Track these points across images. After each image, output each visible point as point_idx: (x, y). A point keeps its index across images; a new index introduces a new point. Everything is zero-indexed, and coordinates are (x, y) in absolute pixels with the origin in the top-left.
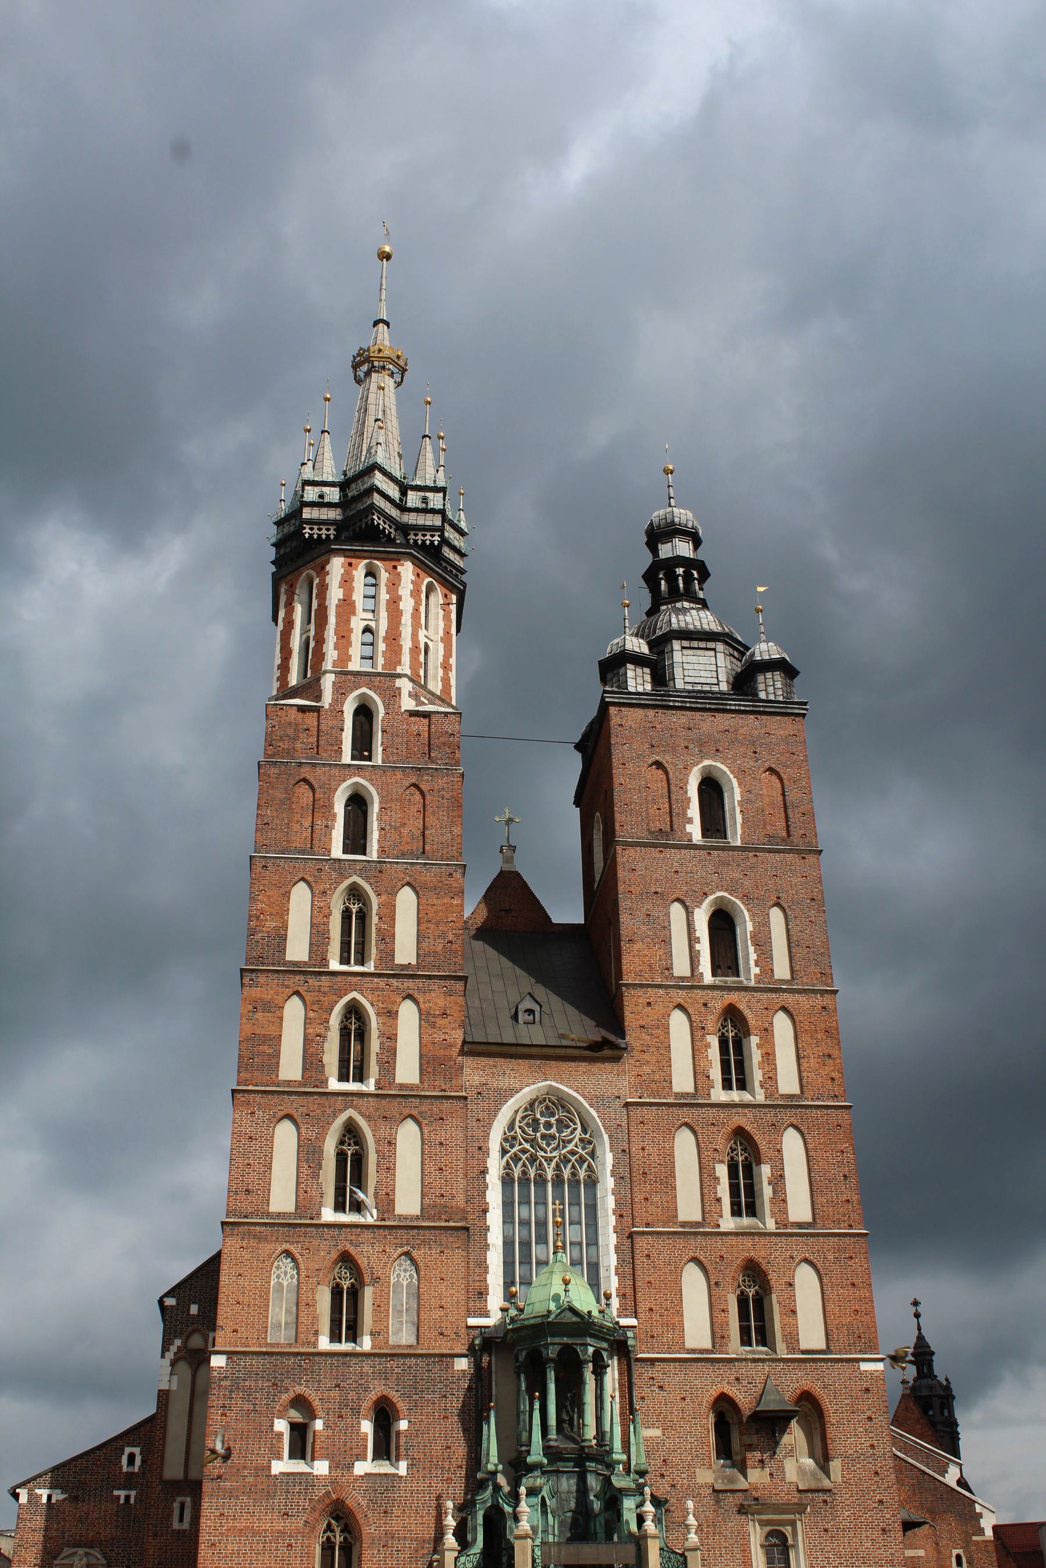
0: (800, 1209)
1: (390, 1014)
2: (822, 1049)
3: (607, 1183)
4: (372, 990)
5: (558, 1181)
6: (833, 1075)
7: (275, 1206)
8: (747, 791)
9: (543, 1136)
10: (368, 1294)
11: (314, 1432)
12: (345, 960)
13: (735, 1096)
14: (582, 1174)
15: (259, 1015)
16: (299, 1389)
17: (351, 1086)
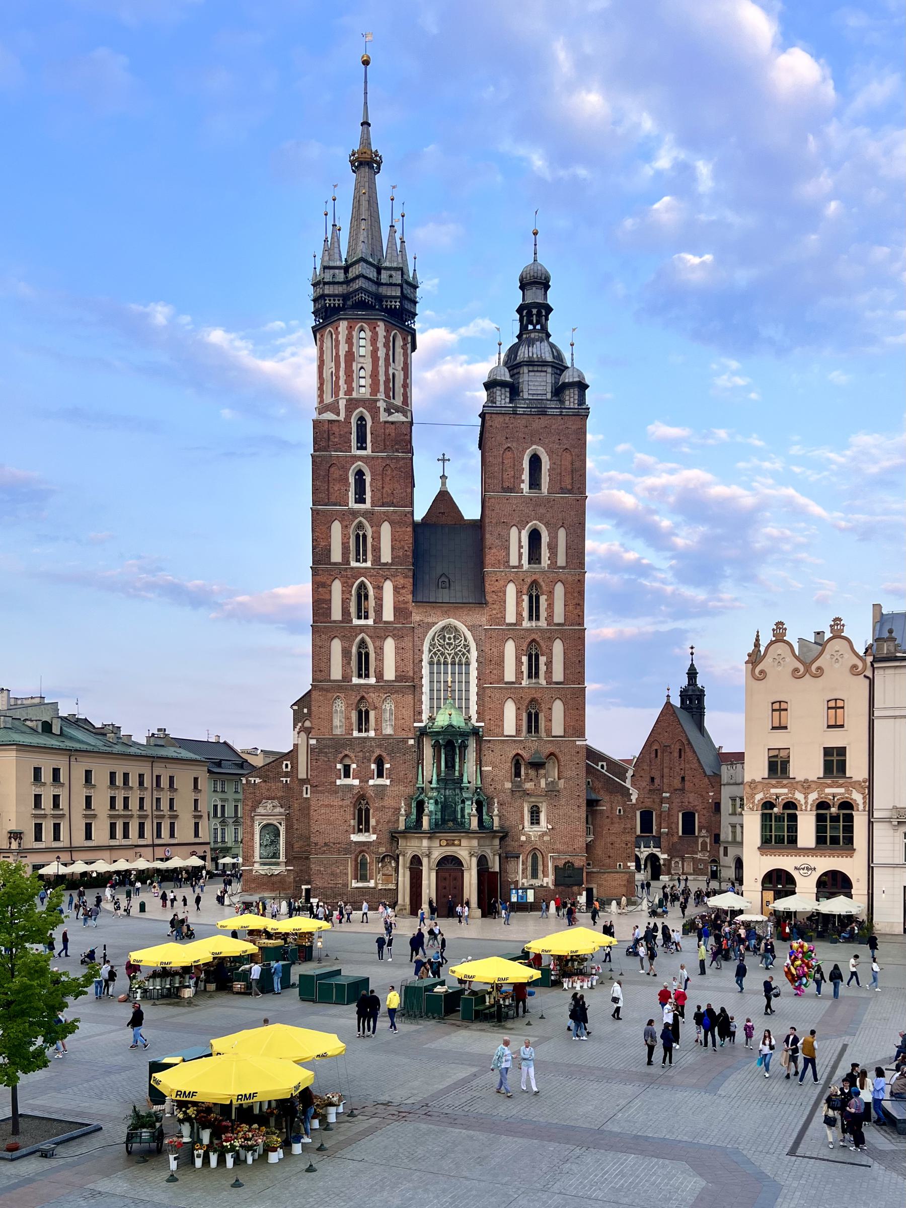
0: (558, 675)
1: (379, 588)
2: (576, 601)
3: (474, 665)
4: (371, 576)
5: (453, 664)
6: (580, 614)
7: (332, 678)
8: (553, 463)
9: (447, 644)
10: (372, 714)
11: (354, 769)
12: (358, 560)
13: (534, 623)
14: (464, 660)
15: (320, 589)
16: (347, 752)
17: (362, 622)
